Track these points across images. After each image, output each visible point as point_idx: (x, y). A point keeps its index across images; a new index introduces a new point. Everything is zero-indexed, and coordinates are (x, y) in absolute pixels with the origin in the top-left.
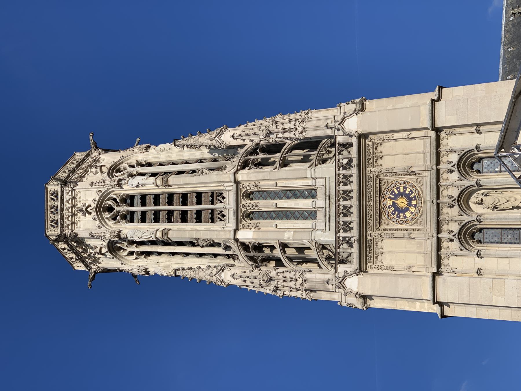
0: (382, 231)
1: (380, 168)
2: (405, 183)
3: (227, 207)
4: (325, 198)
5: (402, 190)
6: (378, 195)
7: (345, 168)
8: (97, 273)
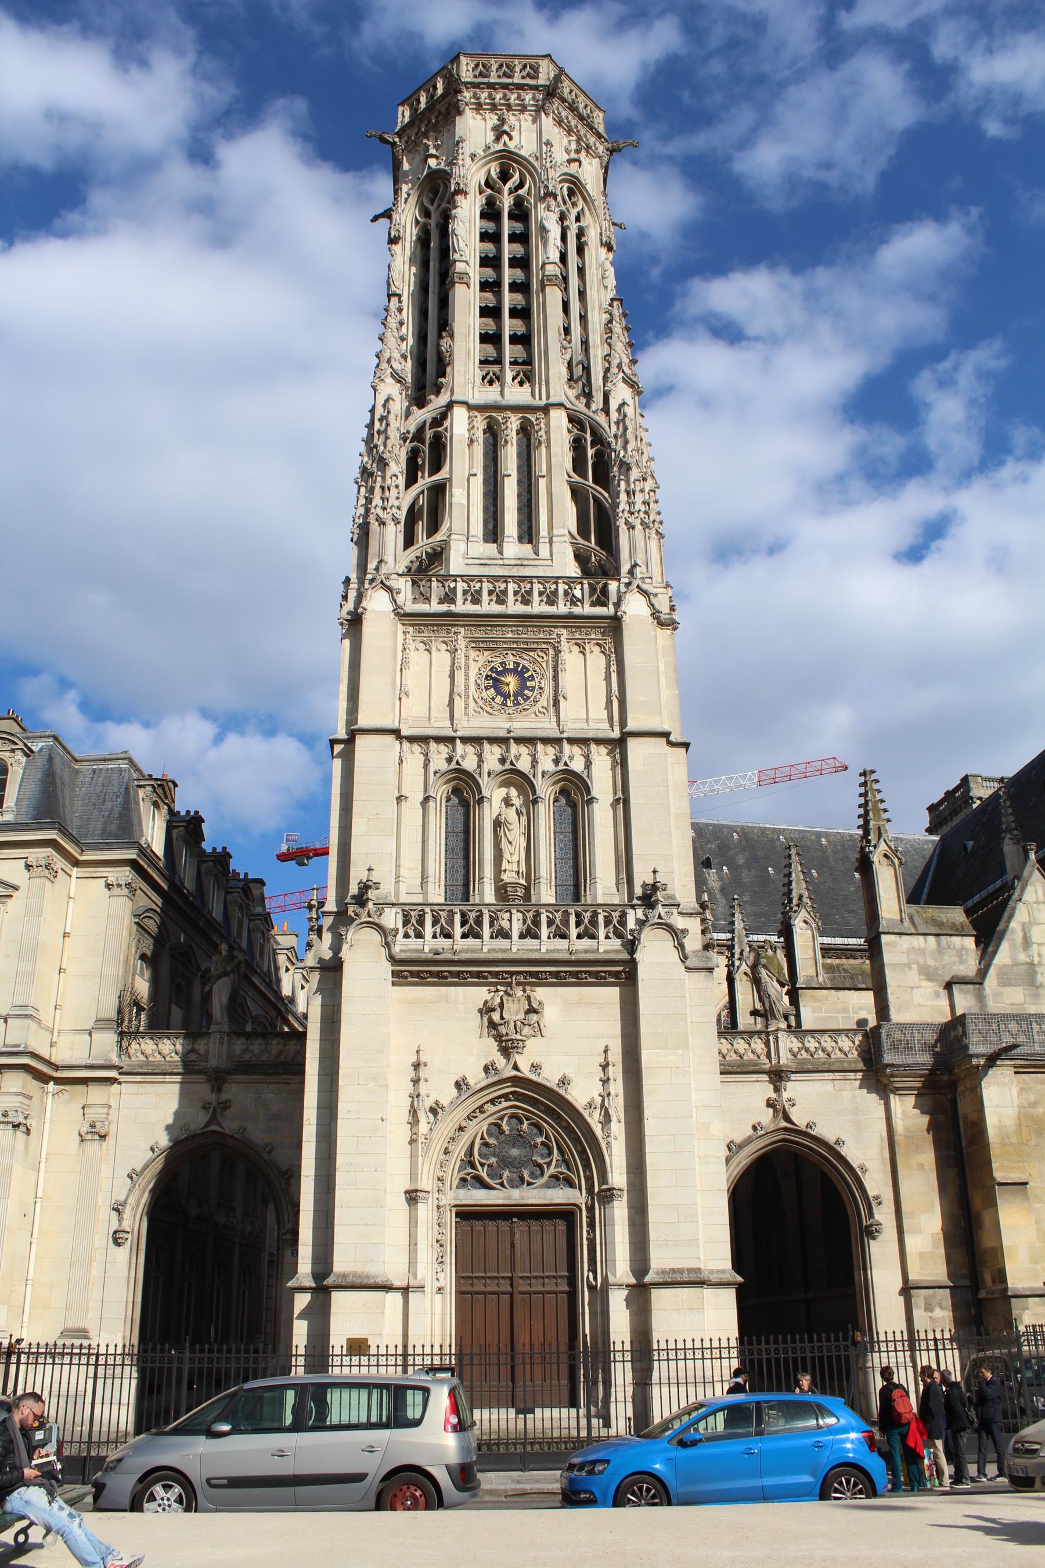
0: (464, 651)
1: (567, 650)
2: (541, 688)
3: (506, 390)
4: (519, 559)
5: (529, 684)
6: (522, 646)
7: (566, 593)
8: (392, 147)
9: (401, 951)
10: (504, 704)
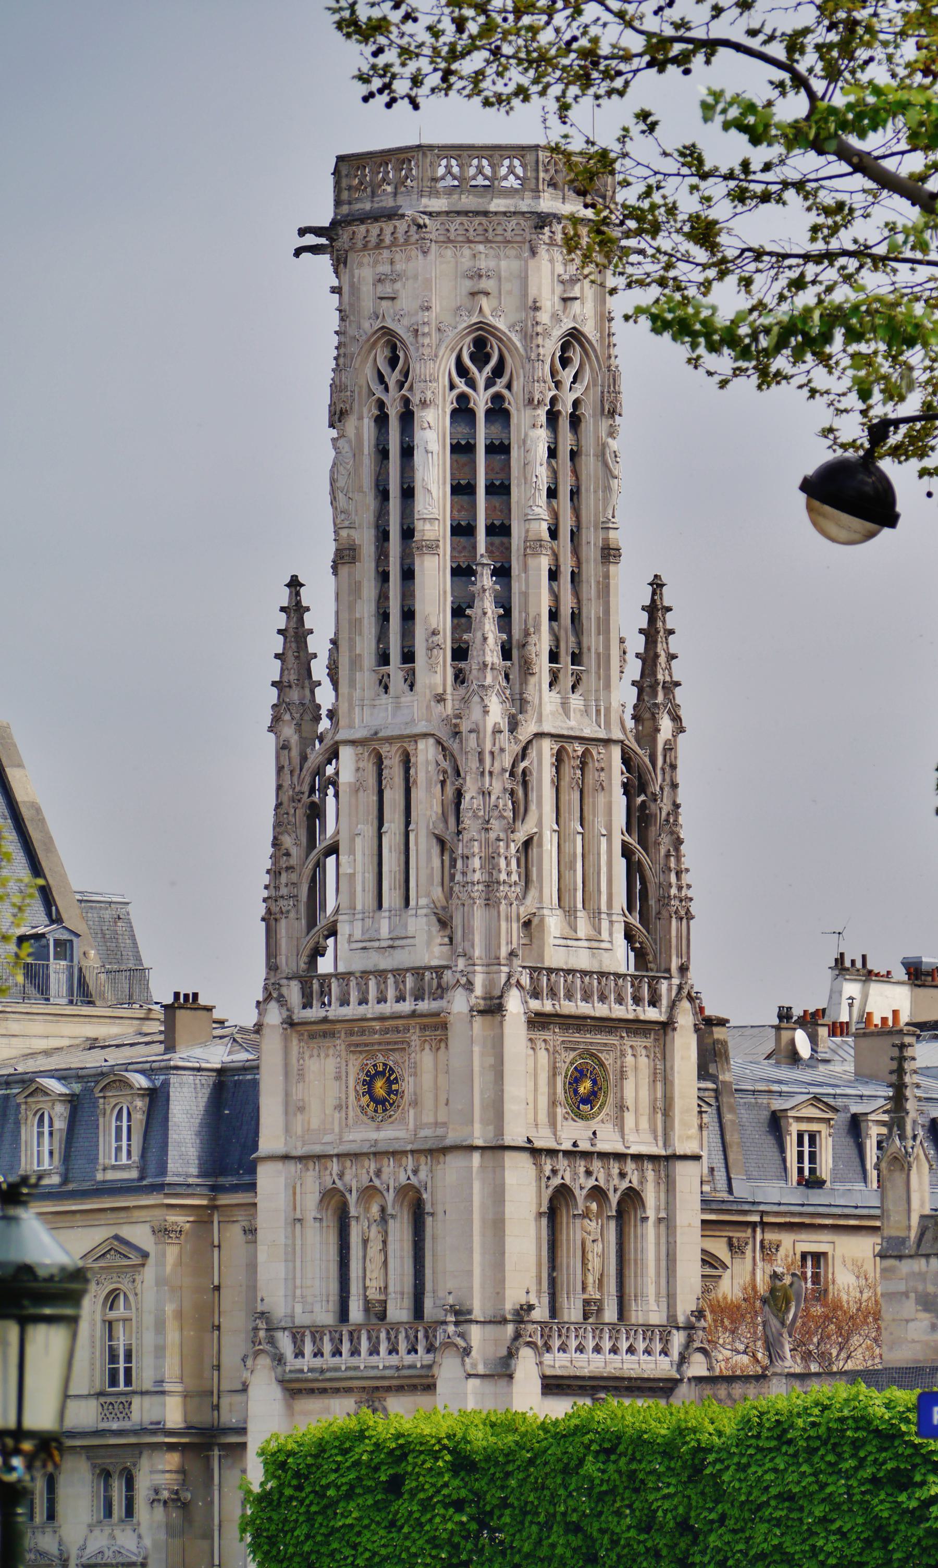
9: (291, 1371)
10: (376, 1111)
